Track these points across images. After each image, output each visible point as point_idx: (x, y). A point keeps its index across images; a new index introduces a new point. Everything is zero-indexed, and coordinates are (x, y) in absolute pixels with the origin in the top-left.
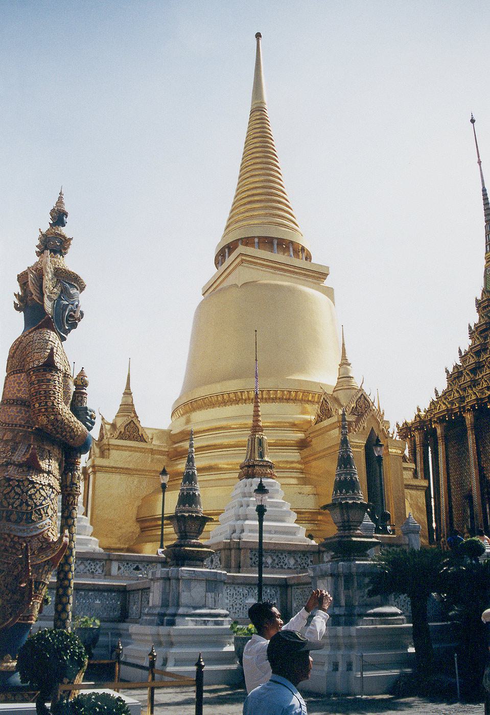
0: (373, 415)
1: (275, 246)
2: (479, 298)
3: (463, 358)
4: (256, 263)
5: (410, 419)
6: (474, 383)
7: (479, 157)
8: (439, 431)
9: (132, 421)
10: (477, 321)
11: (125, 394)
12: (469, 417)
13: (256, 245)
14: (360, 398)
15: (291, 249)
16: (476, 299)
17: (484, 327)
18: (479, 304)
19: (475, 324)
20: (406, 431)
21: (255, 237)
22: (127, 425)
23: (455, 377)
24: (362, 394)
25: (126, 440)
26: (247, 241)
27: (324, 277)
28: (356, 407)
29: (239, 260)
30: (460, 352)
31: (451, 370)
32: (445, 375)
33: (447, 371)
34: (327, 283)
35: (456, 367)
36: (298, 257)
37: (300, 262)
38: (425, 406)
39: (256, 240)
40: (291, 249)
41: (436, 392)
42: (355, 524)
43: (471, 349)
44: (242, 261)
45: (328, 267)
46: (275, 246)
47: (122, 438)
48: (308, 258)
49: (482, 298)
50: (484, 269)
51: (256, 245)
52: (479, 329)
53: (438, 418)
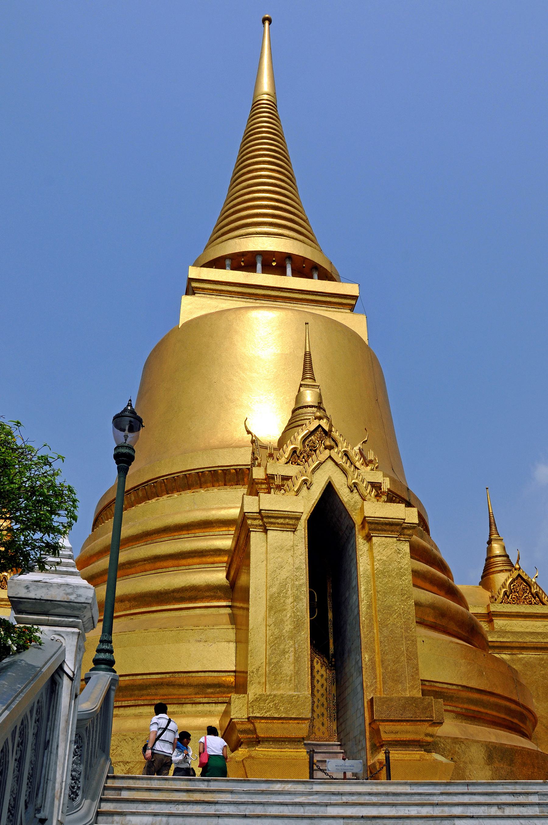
0: (330, 457)
1: (259, 266)
14: (312, 433)
24: (320, 426)
39: (228, 262)
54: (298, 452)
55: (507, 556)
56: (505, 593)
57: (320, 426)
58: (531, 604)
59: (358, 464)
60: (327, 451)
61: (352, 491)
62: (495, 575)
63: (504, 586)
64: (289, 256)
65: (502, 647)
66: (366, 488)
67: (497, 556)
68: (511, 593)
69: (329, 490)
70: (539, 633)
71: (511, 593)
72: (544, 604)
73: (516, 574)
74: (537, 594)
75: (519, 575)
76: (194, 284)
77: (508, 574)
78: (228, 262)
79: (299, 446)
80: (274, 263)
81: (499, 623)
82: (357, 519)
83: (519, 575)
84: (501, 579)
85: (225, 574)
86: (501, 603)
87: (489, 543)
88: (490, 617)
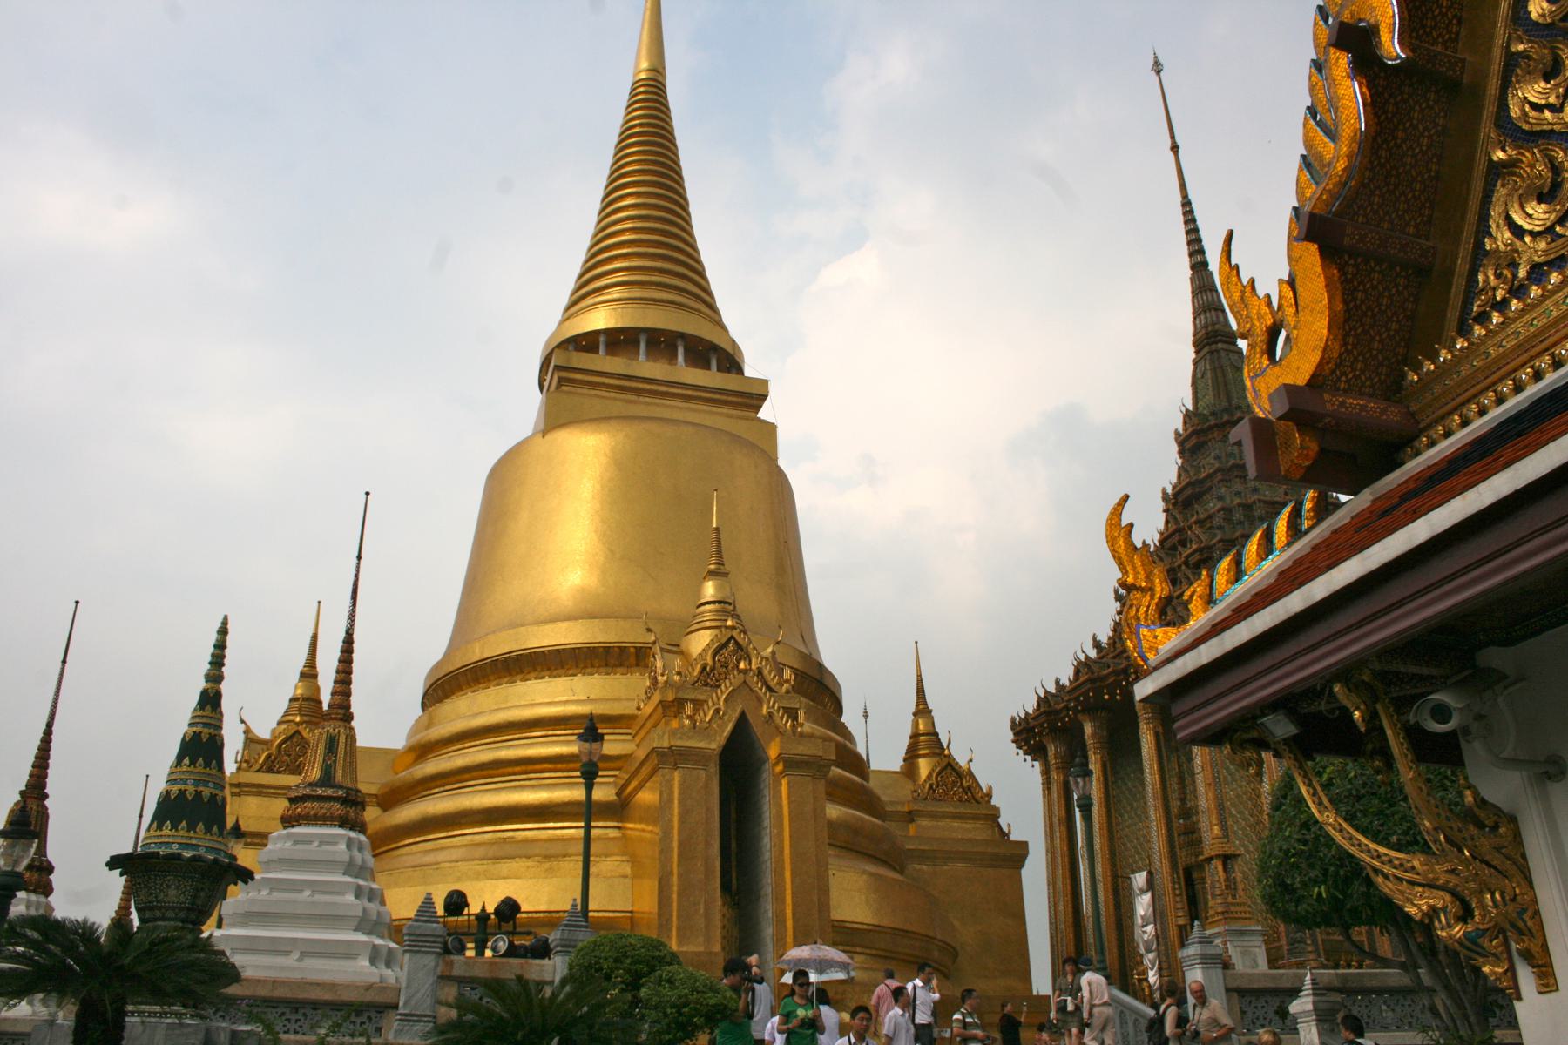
2: (1181, 430)
5: (1031, 706)
7: (1173, 137)
8: (1088, 729)
9: (297, 732)
10: (1174, 480)
11: (303, 675)
14: (724, 646)
15: (681, 351)
17: (1189, 492)
18: (1182, 441)
21: (597, 332)
22: (284, 741)
25: (279, 772)
28: (713, 669)
34: (765, 413)
36: (707, 367)
37: (710, 378)
39: (602, 339)
40: (681, 351)
41: (1097, 644)
42: (170, 914)
44: (561, 380)
45: (765, 383)
47: (270, 770)
53: (1077, 699)
55: (937, 734)
59: (772, 684)
63: (929, 777)
64: (683, 336)
65: (922, 856)
69: (742, 723)
70: (970, 840)
73: (945, 761)
74: (969, 788)
78: (602, 339)
79: (709, 661)
80: (661, 343)
81: (924, 822)
82: (773, 751)
83: (949, 764)
84: (924, 767)
85: (614, 791)
88: (910, 817)
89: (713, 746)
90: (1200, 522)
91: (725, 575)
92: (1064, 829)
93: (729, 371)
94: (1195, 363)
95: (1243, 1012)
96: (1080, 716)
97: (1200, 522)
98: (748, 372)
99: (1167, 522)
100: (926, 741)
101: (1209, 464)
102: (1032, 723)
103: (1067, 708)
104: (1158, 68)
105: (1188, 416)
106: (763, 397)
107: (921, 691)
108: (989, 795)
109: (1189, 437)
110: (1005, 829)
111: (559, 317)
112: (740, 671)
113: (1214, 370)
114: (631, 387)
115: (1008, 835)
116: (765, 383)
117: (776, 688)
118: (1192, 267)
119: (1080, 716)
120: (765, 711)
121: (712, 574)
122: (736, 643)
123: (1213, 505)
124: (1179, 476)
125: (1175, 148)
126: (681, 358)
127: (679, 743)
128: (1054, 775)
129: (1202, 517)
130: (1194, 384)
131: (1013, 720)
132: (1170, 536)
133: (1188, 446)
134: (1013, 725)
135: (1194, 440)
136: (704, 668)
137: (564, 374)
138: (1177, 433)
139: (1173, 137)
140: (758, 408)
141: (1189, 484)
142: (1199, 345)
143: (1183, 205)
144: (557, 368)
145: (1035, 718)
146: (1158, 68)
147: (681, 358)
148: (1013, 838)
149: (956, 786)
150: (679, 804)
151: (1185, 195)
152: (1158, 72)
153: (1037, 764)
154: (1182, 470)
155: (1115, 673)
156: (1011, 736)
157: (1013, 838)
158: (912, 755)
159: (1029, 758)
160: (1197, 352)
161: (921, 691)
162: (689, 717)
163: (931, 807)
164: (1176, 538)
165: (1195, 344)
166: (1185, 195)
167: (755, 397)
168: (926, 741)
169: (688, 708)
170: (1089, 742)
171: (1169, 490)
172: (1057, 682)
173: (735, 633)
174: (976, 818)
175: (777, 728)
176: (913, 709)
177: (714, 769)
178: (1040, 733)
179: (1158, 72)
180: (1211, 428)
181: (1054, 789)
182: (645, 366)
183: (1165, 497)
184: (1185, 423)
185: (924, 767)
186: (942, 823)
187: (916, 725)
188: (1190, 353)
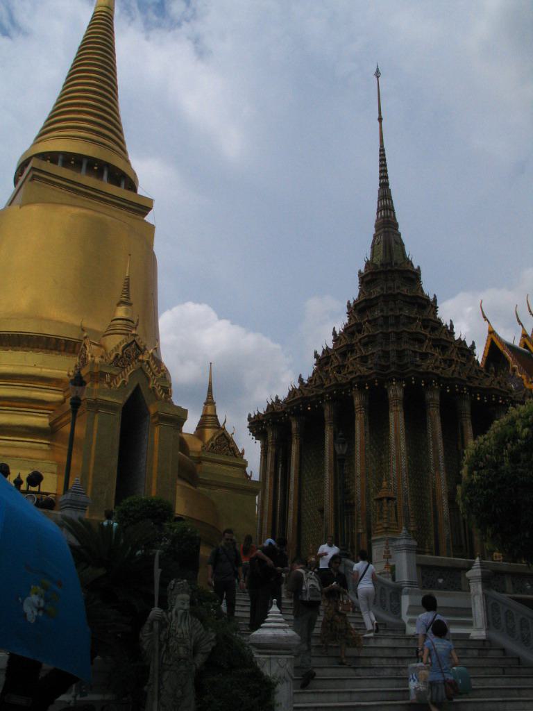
0: (141, 368)
1: (84, 167)
2: (363, 270)
3: (337, 339)
4: (54, 183)
6: (340, 369)
7: (380, 113)
8: (294, 425)
10: (356, 297)
12: (328, 412)
13: (60, 163)
15: (106, 173)
16: (360, 272)
19: (355, 301)
20: (258, 426)
23: (323, 360)
24: (134, 341)
26: (52, 157)
27: (144, 211)
29: (30, 176)
30: (334, 333)
31: (320, 353)
32: (315, 361)
33: (316, 356)
34: (149, 218)
35: (326, 351)
36: (119, 185)
37: (120, 191)
38: (283, 395)
39: (61, 157)
40: (106, 173)
41: (301, 380)
43: (345, 329)
44: (34, 176)
46: (84, 167)
48: (132, 185)
49: (366, 271)
50: (372, 238)
51: (60, 163)
52: (358, 308)
54: (119, 357)
55: (216, 416)
56: (212, 444)
57: (134, 341)
58: (227, 455)
59: (155, 371)
60: (139, 364)
61: (151, 392)
62: (207, 430)
63: (212, 439)
64: (108, 165)
66: (159, 391)
67: (209, 416)
68: (216, 445)
69: (137, 389)
71: (216, 445)
72: (236, 456)
73: (221, 432)
75: (223, 434)
76: (36, 173)
77: (217, 430)
78: (61, 157)
79: (120, 353)
80: (96, 167)
81: (206, 464)
82: (152, 410)
83: (223, 434)
84: (209, 433)
86: (208, 451)
87: (205, 404)
88: (199, 460)
89: (121, 402)
90: (369, 321)
91: (130, 304)
92: (272, 477)
93: (129, 189)
94: (375, 237)
95: (423, 578)
96: (291, 418)
97: (369, 321)
98: (140, 192)
99: (350, 320)
100: (209, 420)
101: (376, 291)
102: (261, 418)
103: (284, 412)
104: (378, 74)
105: (368, 264)
106: (149, 209)
107: (210, 390)
108: (243, 453)
109: (367, 275)
110: (249, 474)
111: (31, 141)
112: (139, 361)
113: (385, 241)
114: (77, 190)
115: (250, 477)
116: (151, 201)
117: (156, 374)
118: (380, 185)
119: (291, 418)
120: (151, 385)
121: (121, 303)
122: (136, 344)
123: (377, 313)
124: (359, 296)
125: (380, 119)
126: (105, 177)
127: (101, 397)
128: (270, 448)
129: (370, 318)
130: (373, 247)
131: (250, 415)
132: (350, 327)
133: (365, 280)
134: (249, 419)
135: (369, 278)
136: (117, 356)
137: (36, 173)
138: (360, 273)
139: (380, 113)
140: (144, 217)
141: (365, 300)
142: (378, 227)
143: (380, 151)
144: (33, 169)
145: (264, 416)
146: (378, 74)
147: (105, 177)
148: (252, 479)
149: (225, 443)
150: (98, 433)
151: (382, 146)
152: (378, 77)
153: (259, 442)
154: (361, 291)
155: (317, 396)
156: (247, 423)
157: (252, 479)
158: (202, 426)
159: (254, 438)
160: (376, 231)
161: (210, 390)
162: (108, 383)
163: (211, 456)
164: (354, 328)
165: (376, 226)
166: (382, 146)
167: (143, 208)
168: (209, 420)
169: (108, 378)
170: (294, 432)
171: (352, 302)
172: (277, 398)
173: (136, 338)
174: (234, 465)
175: (156, 396)
176: (205, 400)
177: (118, 415)
178: (266, 425)
179: (378, 77)
180: (380, 272)
181: (269, 455)
182: (85, 179)
183: (349, 306)
184: (366, 267)
185: (209, 433)
186: (217, 466)
187: (205, 410)
188: (372, 231)
